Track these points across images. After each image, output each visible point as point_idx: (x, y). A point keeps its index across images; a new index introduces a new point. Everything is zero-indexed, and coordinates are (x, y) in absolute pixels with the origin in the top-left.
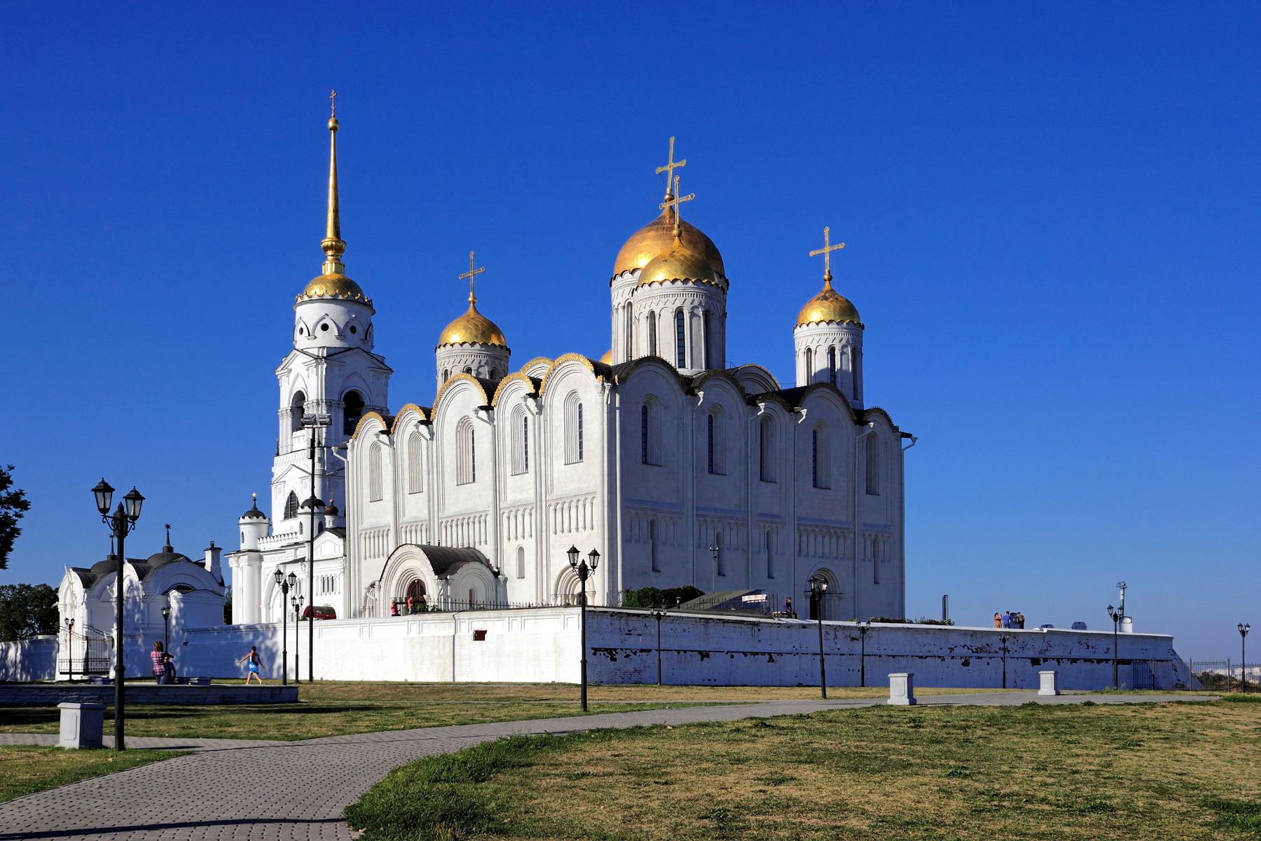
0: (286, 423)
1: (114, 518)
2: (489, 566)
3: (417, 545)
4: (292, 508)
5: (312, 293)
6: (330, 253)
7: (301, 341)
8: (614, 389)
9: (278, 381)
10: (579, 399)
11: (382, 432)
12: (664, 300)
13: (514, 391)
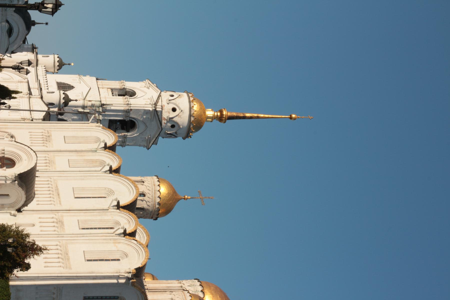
0: (117, 85)
3: (36, 164)
4: (63, 87)
5: (195, 103)
6: (219, 114)
7: (166, 95)
8: (128, 279)
9: (143, 81)
10: (123, 258)
11: (106, 144)
13: (127, 221)
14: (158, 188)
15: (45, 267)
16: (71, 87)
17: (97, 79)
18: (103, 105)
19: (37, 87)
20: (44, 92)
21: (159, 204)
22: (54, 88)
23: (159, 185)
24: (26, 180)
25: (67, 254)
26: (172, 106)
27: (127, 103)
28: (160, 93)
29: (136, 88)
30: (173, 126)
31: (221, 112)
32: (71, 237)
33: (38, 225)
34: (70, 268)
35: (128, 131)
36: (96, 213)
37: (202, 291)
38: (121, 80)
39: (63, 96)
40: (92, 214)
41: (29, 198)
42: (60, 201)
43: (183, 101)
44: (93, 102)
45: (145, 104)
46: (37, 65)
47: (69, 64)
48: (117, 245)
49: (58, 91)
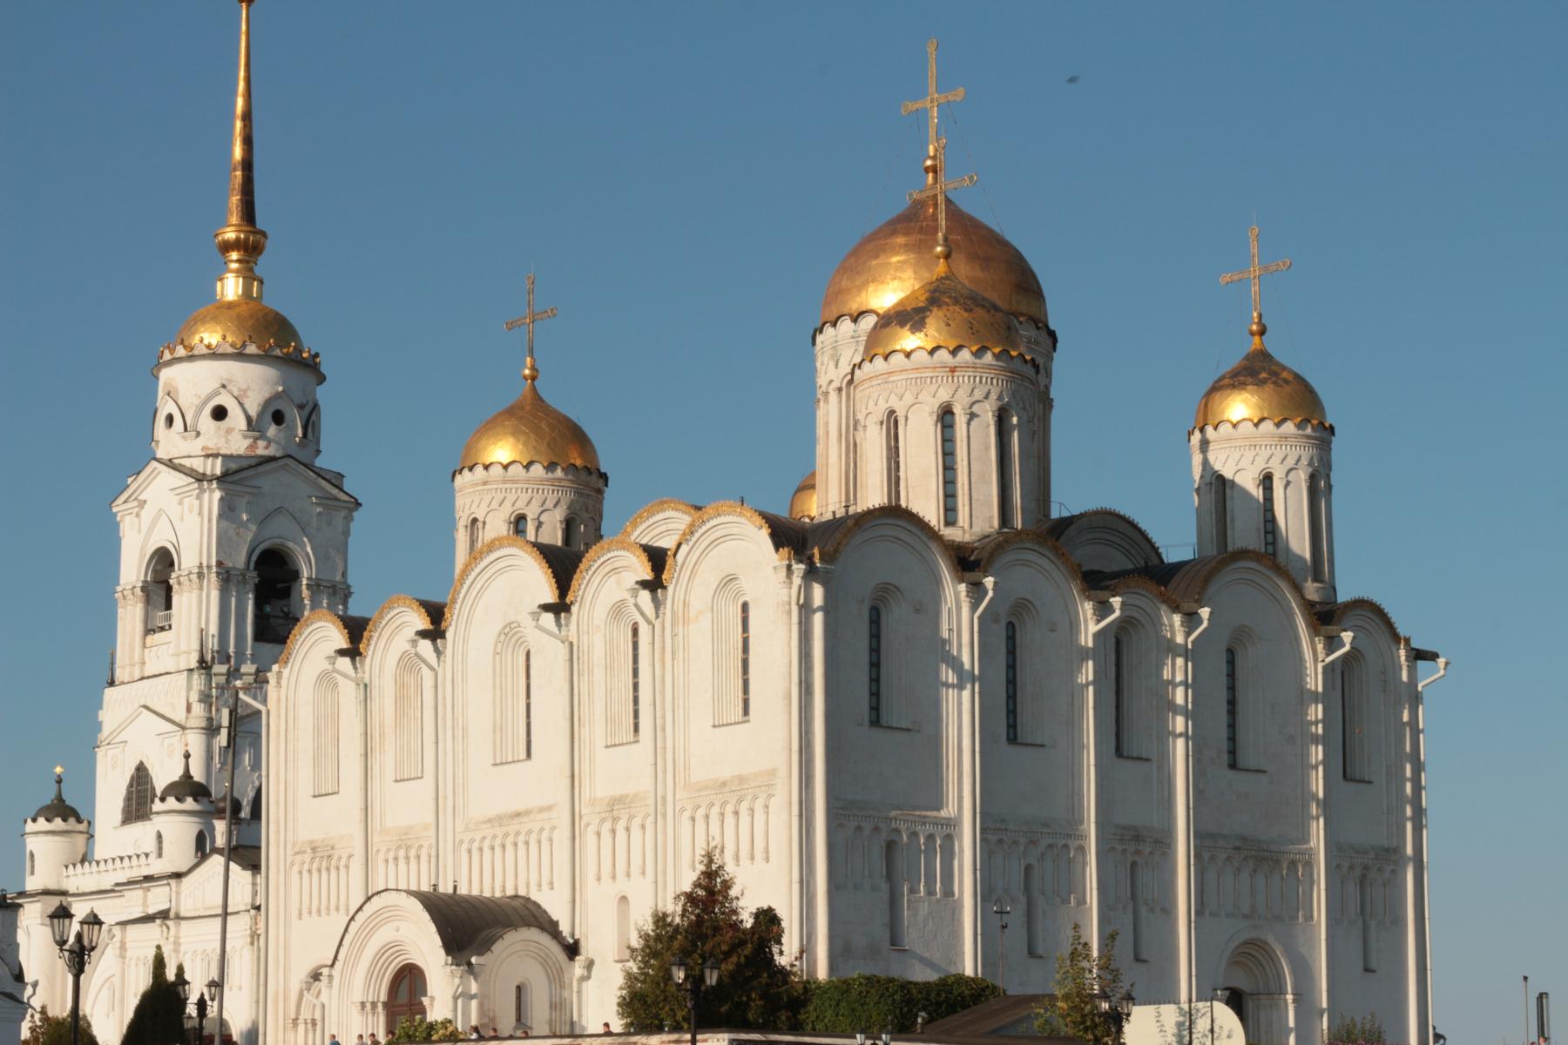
0: (130, 615)
1: (71, 952)
4: (139, 802)
6: (234, 255)
7: (169, 442)
8: (811, 574)
9: (118, 524)
10: (739, 593)
11: (342, 653)
13: (611, 577)
14: (496, 471)
15: (767, 860)
16: (141, 775)
17: (112, 683)
18: (202, 661)
19: (140, 892)
20: (157, 867)
21: (551, 467)
22: (142, 834)
23: (486, 467)
24: (467, 926)
25: (724, 784)
27: (194, 577)
28: (159, 461)
29: (143, 548)
30: (278, 418)
31: (226, 247)
32: (665, 771)
33: (623, 887)
34: (773, 773)
35: (296, 575)
36: (582, 686)
37: (855, 320)
38: (115, 602)
39: (171, 802)
40: (585, 698)
41: (527, 915)
42: (541, 810)
43: (189, 383)
44: (194, 697)
45: (200, 513)
46: (64, 893)
47: (59, 782)
48: (692, 614)
49: (156, 819)
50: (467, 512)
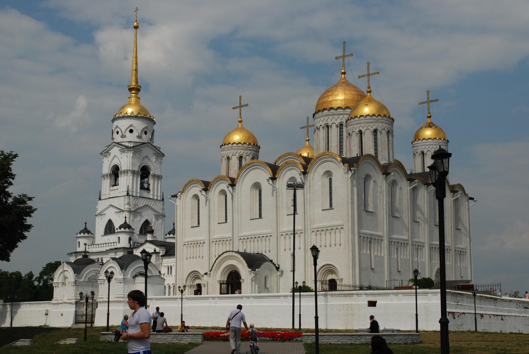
0: (106, 183)
2: (275, 265)
3: (238, 252)
4: (110, 229)
12: (367, 125)
15: (340, 245)
16: (110, 222)
17: (100, 199)
18: (128, 194)
20: (119, 246)
22: (112, 238)
24: (255, 261)
26: (128, 133)
29: (110, 165)
39: (123, 230)
44: (126, 202)
50: (226, 155)
